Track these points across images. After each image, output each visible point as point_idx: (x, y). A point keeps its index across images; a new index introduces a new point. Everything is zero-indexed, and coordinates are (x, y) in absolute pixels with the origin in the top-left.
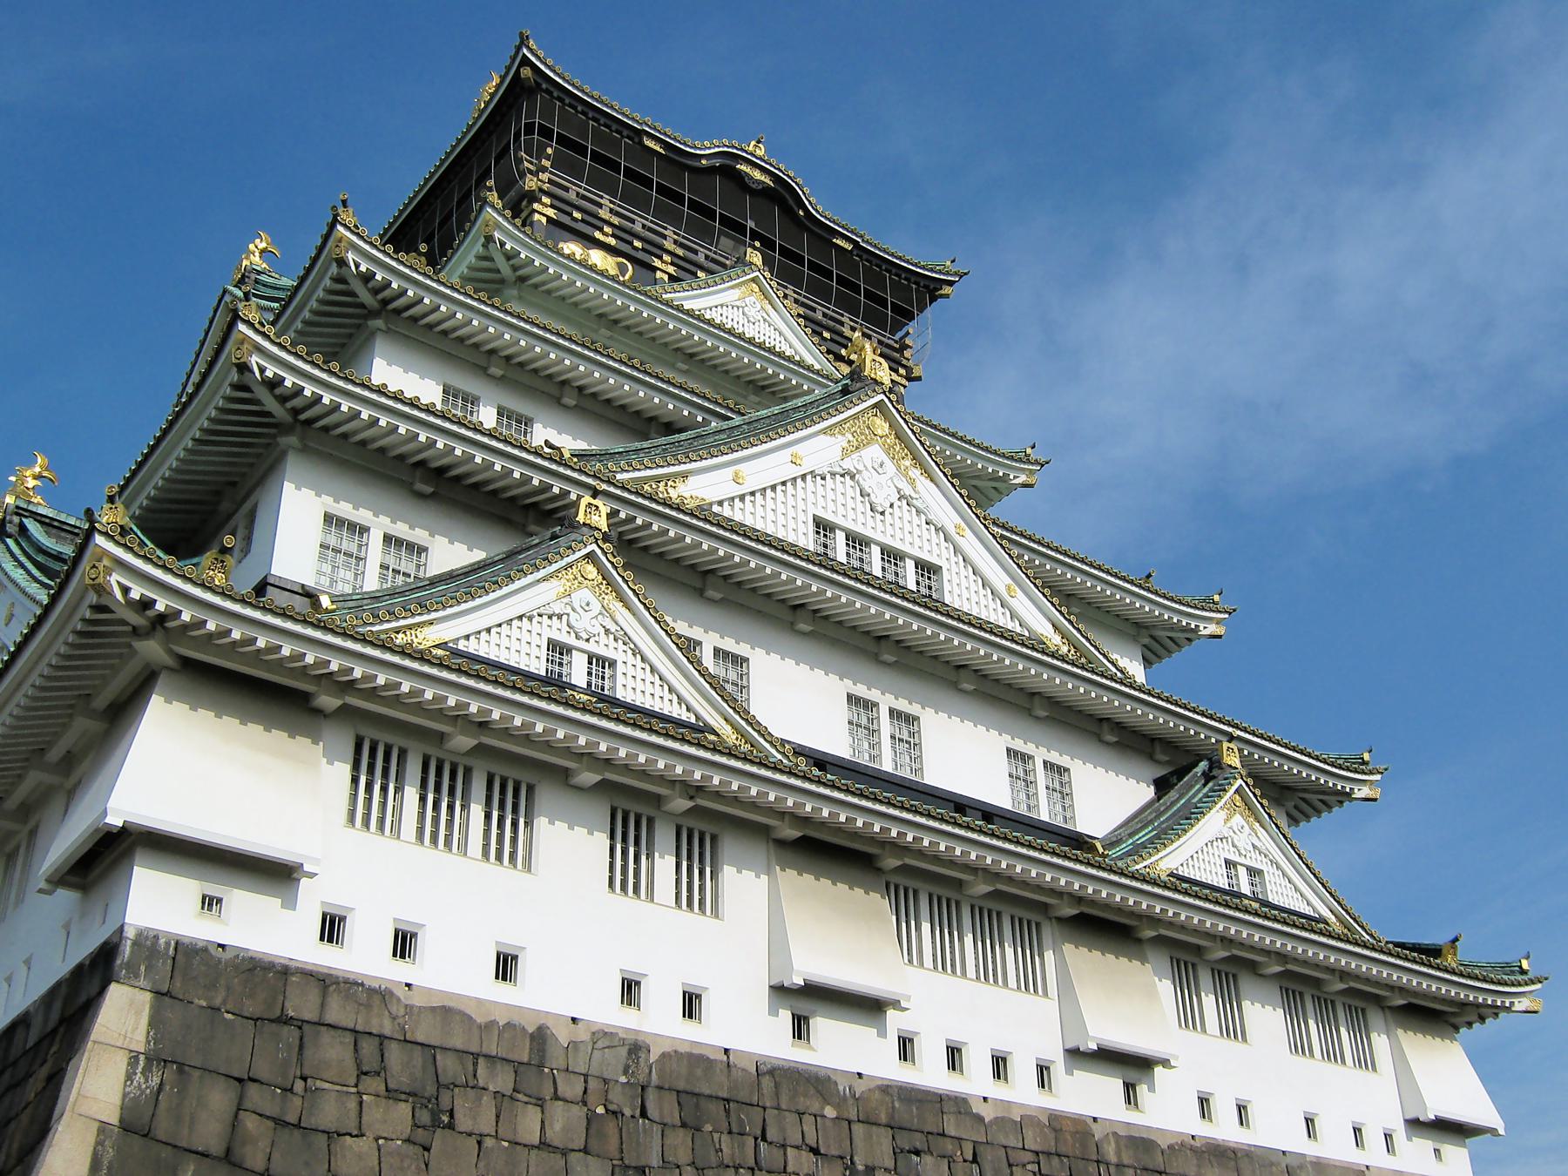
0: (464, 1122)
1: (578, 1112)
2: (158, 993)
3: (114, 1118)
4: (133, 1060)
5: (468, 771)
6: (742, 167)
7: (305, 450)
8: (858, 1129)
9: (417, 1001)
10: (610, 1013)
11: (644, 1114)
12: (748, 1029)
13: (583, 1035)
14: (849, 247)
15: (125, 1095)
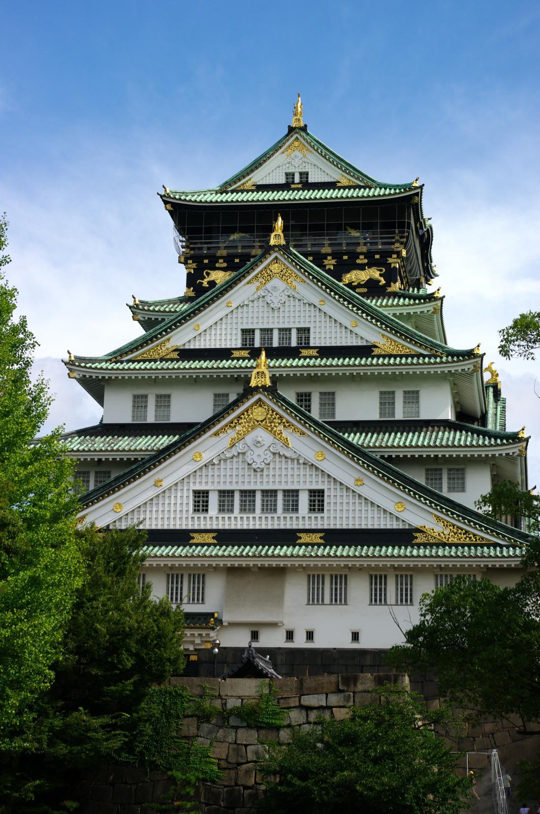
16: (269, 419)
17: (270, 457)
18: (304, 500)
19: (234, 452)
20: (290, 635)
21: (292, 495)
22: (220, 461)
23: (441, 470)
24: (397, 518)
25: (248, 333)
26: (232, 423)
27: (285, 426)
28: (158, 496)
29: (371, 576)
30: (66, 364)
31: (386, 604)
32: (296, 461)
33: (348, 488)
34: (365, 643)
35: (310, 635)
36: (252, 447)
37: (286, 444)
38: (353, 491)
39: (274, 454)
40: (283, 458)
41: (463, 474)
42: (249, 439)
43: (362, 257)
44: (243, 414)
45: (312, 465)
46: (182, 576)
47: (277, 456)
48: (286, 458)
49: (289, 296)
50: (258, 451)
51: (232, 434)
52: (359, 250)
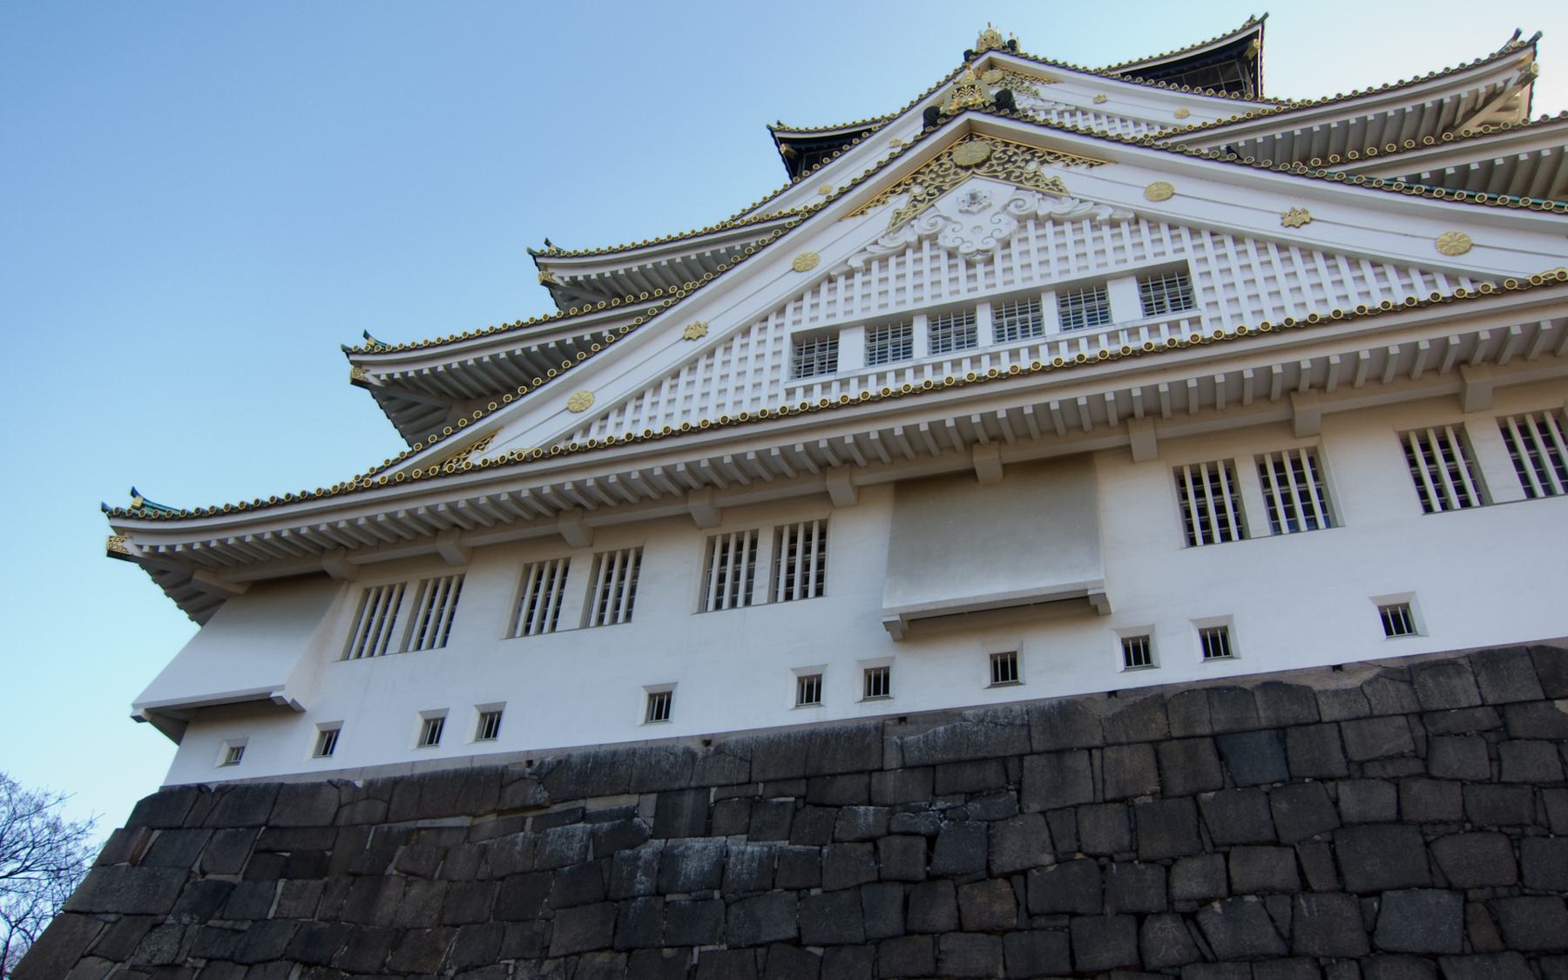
17: (1007, 226)
18: (1125, 303)
19: (908, 235)
22: (868, 263)
26: (899, 185)
28: (692, 364)
32: (1086, 224)
33: (1262, 243)
35: (1216, 643)
36: (956, 217)
37: (1055, 190)
38: (1282, 246)
39: (1022, 220)
40: (1049, 225)
47: (1031, 224)
48: (1057, 222)
50: (969, 222)
51: (900, 202)
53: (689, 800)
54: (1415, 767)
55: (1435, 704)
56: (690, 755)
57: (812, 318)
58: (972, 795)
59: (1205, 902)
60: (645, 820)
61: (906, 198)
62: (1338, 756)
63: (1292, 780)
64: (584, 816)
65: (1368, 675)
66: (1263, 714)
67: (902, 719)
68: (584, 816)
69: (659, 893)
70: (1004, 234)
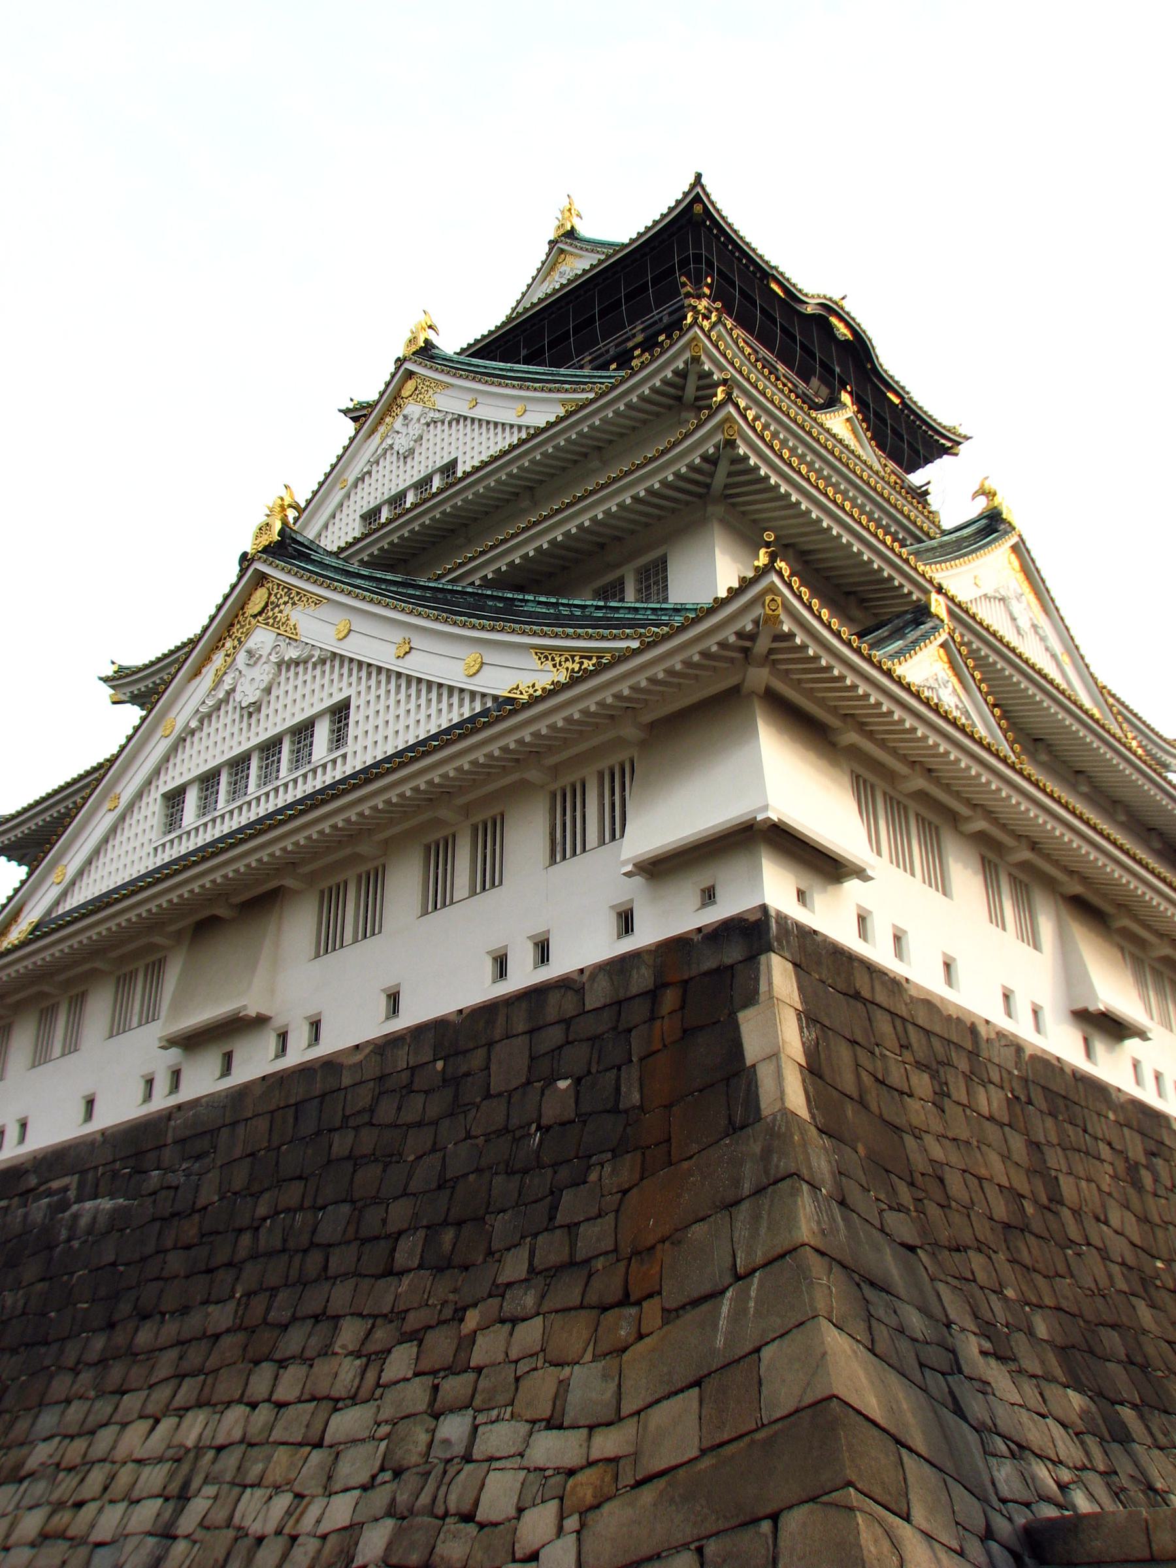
0: (955, 1096)
1: (1001, 1094)
2: (795, 965)
3: (803, 1063)
4: (799, 1019)
5: (905, 808)
6: (834, 320)
7: (723, 521)
8: (1126, 1130)
9: (913, 992)
10: (1001, 1021)
11: (1030, 1102)
12: (1063, 1043)
13: (993, 1036)
14: (897, 401)
15: (803, 1044)
16: (272, 603)
20: (283, 1037)
21: (303, 731)
22: (201, 721)
23: (621, 582)
24: (473, 694)
25: (370, 516)
27: (294, 604)
29: (428, 848)
30: (106, 680)
31: (452, 903)
34: (412, 1015)
41: (665, 570)
42: (241, 657)
43: (637, 353)
44: (237, 616)
45: (334, 654)
46: (137, 970)
49: (428, 425)
50: (249, 673)
51: (219, 659)
52: (630, 344)
53: (90, 1176)
54: (366, 1118)
55: (387, 1071)
56: (93, 1143)
57: (168, 783)
58: (198, 1158)
59: (264, 1219)
60: (72, 1194)
61: (222, 653)
62: (340, 1113)
63: (318, 1133)
64: (50, 1193)
65: (367, 1051)
66: (318, 1088)
67: (179, 1107)
68: (50, 1193)
69: (69, 1240)
70: (263, 686)
